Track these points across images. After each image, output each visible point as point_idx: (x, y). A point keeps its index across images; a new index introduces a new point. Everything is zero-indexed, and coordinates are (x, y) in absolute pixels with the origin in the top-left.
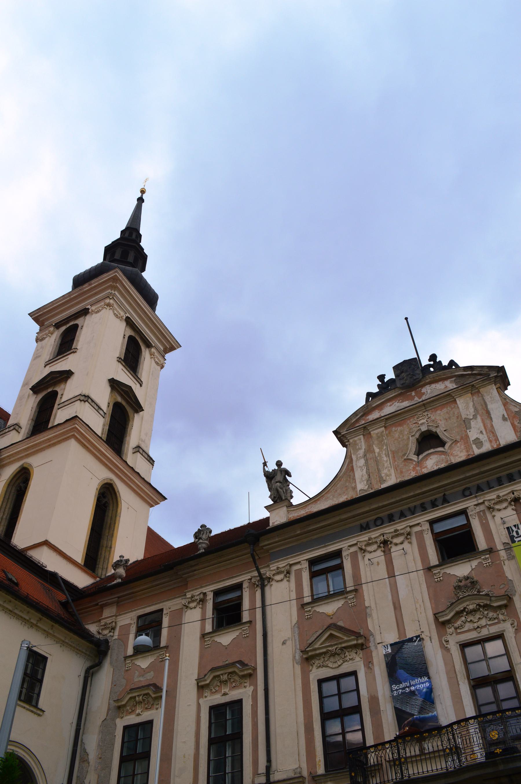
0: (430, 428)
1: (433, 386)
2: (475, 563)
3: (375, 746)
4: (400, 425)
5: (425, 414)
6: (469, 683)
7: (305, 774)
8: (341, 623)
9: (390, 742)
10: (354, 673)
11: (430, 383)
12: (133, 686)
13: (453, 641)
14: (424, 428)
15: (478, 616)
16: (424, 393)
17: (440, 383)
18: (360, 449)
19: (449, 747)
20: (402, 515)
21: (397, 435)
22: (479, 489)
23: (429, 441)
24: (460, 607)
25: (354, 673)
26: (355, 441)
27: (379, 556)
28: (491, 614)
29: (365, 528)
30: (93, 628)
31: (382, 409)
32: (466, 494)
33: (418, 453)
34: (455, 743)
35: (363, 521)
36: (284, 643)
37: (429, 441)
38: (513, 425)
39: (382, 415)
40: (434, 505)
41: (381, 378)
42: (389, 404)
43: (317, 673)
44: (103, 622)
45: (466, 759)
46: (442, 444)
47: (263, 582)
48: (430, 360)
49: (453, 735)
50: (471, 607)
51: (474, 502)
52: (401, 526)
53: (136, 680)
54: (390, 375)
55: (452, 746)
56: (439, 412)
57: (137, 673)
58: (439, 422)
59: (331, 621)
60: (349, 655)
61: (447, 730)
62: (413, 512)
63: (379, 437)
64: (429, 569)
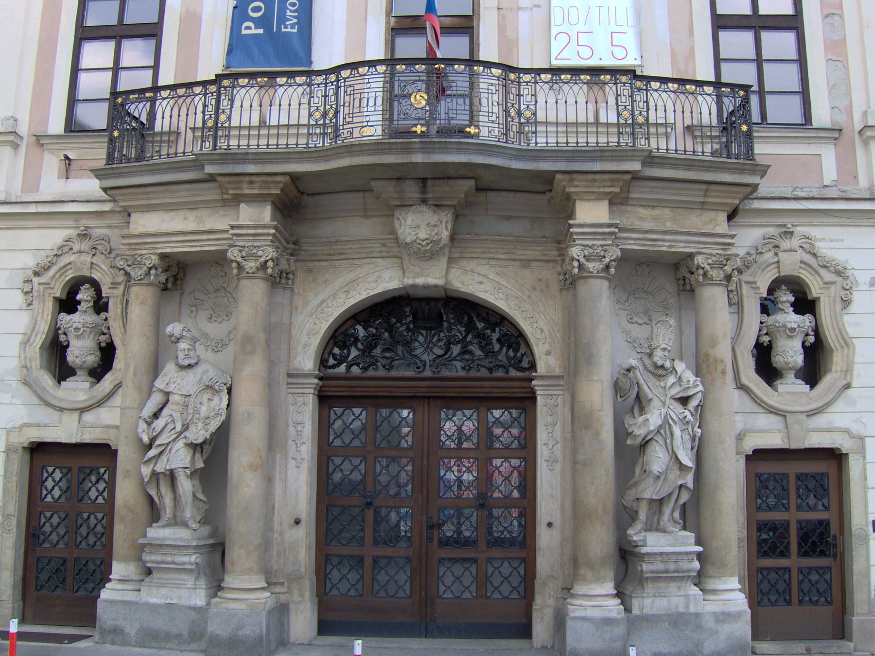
3: (173, 87)
6: (388, 23)
7: (23, 129)
9: (204, 84)
19: (322, 108)
34: (337, 104)
45: (352, 133)
49: (338, 87)
55: (328, 107)
61: (326, 79)
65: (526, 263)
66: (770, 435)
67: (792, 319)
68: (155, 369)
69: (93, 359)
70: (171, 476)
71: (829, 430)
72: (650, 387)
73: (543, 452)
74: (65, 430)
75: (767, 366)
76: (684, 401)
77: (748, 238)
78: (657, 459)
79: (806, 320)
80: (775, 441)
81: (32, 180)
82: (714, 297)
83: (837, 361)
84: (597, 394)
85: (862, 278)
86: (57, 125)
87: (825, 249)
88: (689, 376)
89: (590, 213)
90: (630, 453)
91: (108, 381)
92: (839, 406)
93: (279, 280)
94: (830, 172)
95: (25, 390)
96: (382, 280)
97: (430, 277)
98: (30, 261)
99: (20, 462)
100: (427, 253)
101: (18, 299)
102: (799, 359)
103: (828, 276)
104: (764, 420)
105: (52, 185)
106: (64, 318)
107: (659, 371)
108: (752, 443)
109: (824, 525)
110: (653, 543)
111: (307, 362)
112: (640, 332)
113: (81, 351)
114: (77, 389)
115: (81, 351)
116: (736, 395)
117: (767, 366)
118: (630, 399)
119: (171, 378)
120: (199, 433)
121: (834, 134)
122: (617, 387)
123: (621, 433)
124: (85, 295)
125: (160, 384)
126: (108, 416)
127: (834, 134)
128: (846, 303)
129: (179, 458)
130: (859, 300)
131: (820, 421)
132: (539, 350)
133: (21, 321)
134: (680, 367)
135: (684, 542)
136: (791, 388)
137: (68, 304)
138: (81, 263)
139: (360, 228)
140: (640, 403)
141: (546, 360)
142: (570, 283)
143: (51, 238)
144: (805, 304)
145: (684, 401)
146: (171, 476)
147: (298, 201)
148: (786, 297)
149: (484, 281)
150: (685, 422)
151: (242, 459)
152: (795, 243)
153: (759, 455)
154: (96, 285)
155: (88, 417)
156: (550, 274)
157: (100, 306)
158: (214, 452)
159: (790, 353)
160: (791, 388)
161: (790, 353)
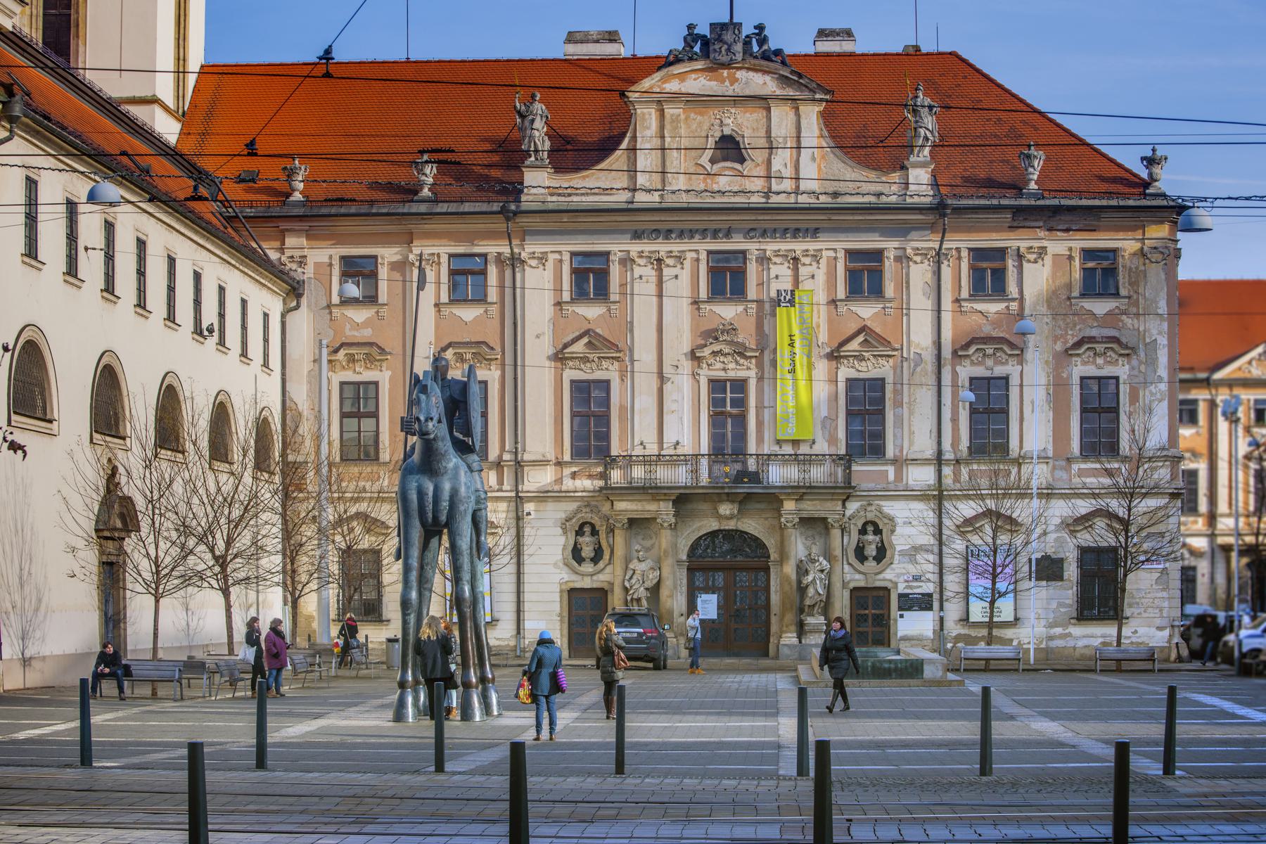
0: (735, 135)
1: (751, 74)
2: (740, 308)
4: (701, 114)
5: (733, 111)
8: (599, 331)
10: (608, 382)
11: (749, 69)
12: (344, 340)
13: (705, 374)
14: (727, 131)
15: (730, 358)
16: (737, 80)
17: (760, 75)
18: (648, 128)
20: (681, 235)
21: (694, 126)
22: (764, 233)
23: (730, 149)
24: (716, 348)
25: (608, 382)
26: (644, 114)
27: (649, 272)
28: (742, 361)
29: (637, 235)
30: (273, 256)
31: (683, 80)
32: (749, 233)
33: (713, 161)
35: (640, 227)
36: (538, 337)
37: (730, 149)
38: (819, 167)
39: (683, 90)
40: (715, 234)
41: (691, 27)
42: (693, 76)
43: (570, 374)
44: (288, 253)
46: (742, 160)
47: (515, 262)
48: (756, 28)
50: (727, 351)
51: (757, 246)
52: (676, 247)
53: (348, 333)
54: (703, 29)
56: (748, 115)
57: (348, 326)
58: (744, 128)
59: (590, 326)
60: (605, 364)
62: (692, 234)
63: (673, 121)
64: (696, 302)
65: (766, 519)
66: (858, 580)
67: (870, 537)
68: (628, 561)
69: (592, 555)
70: (638, 600)
71: (885, 580)
72: (810, 567)
73: (773, 589)
74: (587, 583)
75: (860, 554)
76: (822, 571)
77: (853, 507)
78: (811, 591)
79: (877, 538)
80: (862, 584)
81: (559, 481)
82: (836, 533)
83: (888, 553)
84: (790, 569)
85: (899, 521)
86: (567, 457)
87: (886, 510)
88: (825, 563)
89: (789, 505)
90: (802, 590)
91: (601, 564)
92: (888, 571)
93: (674, 528)
94: (891, 477)
95: (566, 569)
96: (714, 525)
97: (731, 525)
98: (564, 516)
99: (566, 596)
100: (731, 517)
101: (560, 531)
102: (874, 553)
103: (886, 521)
104: (857, 576)
105: (568, 484)
106: (580, 539)
107: (813, 561)
108: (852, 585)
109: (882, 615)
110: (810, 620)
111: (684, 558)
112: (809, 543)
113: (587, 552)
114: (588, 567)
115: (587, 552)
116: (846, 567)
117: (860, 554)
118: (802, 571)
119: (634, 564)
120: (649, 584)
121: (894, 461)
122: (798, 566)
123: (799, 582)
124: (587, 529)
125: (631, 566)
126: (601, 577)
127: (894, 461)
128: (893, 531)
129: (642, 593)
130: (899, 530)
131: (881, 576)
132: (771, 551)
133: (562, 540)
134: (821, 559)
135: (822, 620)
136: (871, 565)
137: (579, 532)
138: (588, 517)
139: (705, 506)
140: (807, 572)
141: (774, 556)
142: (782, 528)
143: (573, 506)
144: (877, 531)
145: (822, 571)
146: (638, 600)
147: (683, 500)
148: (870, 528)
149: (751, 525)
150: (821, 579)
151: (664, 592)
152: (873, 508)
153: (855, 589)
154: (593, 526)
155: (595, 578)
156: (775, 522)
157: (594, 532)
158: (655, 590)
159: (871, 551)
160: (871, 565)
161: (871, 551)
